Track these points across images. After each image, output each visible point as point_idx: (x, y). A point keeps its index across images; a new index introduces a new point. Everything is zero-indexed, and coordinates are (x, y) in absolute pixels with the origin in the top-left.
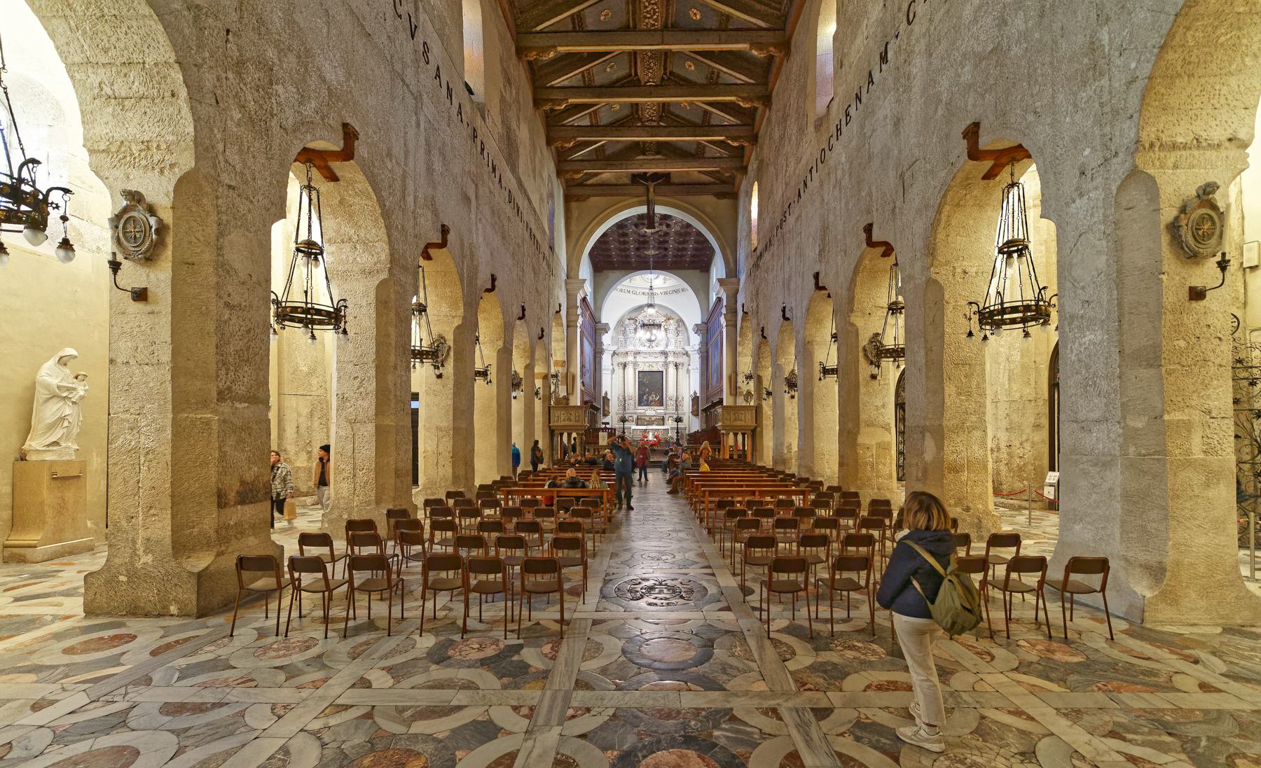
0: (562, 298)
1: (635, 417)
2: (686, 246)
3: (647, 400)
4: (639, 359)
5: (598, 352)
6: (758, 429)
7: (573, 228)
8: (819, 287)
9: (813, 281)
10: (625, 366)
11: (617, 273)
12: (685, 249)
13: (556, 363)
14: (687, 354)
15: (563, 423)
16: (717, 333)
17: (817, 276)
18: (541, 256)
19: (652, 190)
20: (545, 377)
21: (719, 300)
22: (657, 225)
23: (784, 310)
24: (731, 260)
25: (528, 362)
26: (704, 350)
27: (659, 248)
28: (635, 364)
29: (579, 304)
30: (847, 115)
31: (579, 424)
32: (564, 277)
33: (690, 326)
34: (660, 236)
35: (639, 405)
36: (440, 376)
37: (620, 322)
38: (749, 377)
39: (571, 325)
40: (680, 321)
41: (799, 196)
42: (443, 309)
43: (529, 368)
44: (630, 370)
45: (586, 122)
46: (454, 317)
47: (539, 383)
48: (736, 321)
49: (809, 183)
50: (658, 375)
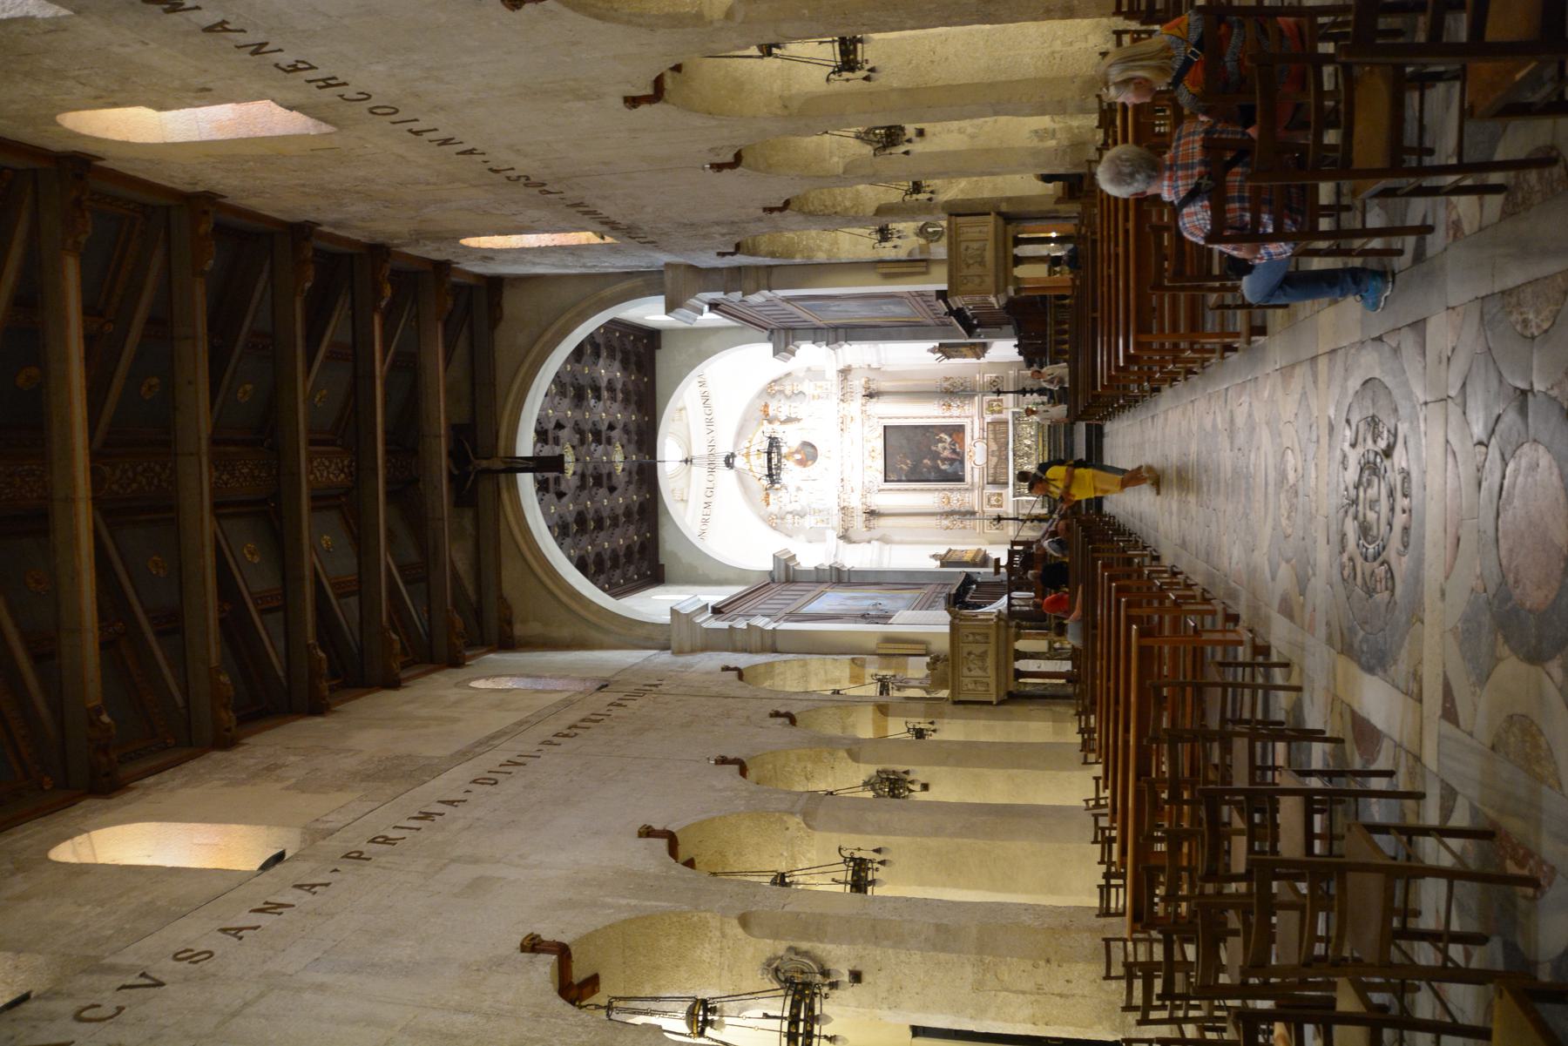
0: (713, 661)
1: (990, 490)
2: (604, 384)
3: (952, 461)
5: (838, 578)
6: (1004, 208)
7: (565, 633)
8: (658, 92)
9: (644, 109)
10: (872, 514)
11: (665, 534)
12: (611, 387)
13: (856, 679)
14: (845, 372)
15: (991, 672)
16: (789, 307)
17: (633, 102)
18: (616, 712)
19: (484, 464)
20: (883, 710)
21: (714, 306)
22: (557, 451)
23: (718, 167)
24: (626, 285)
25: (843, 754)
26: (832, 335)
27: (609, 441)
29: (725, 625)
30: (294, 68)
31: (992, 633)
32: (665, 657)
33: (778, 367)
34: (582, 441)
35: (961, 479)
36: (856, 977)
37: (775, 522)
38: (884, 234)
39: (771, 643)
40: (773, 389)
41: (471, 152)
42: (705, 957)
43: (855, 751)
45: (353, 601)
46: (724, 935)
47: (897, 728)
48: (757, 268)
49: (442, 135)
50: (892, 441)
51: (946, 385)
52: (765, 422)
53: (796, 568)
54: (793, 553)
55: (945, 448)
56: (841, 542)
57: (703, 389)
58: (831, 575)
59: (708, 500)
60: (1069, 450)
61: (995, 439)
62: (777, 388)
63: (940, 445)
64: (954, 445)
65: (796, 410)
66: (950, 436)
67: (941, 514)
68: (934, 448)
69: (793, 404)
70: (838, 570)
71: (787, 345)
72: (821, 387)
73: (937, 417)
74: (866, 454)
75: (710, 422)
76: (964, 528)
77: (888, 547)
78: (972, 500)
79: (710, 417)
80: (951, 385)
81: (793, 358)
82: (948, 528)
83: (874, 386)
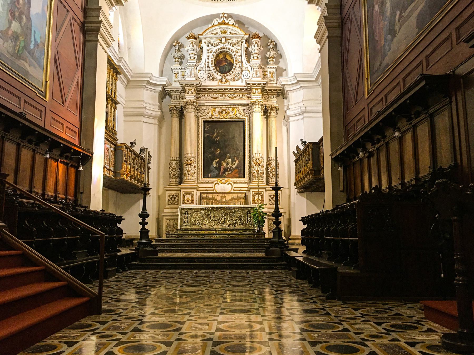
1: (197, 195)
3: (218, 168)
4: (205, 100)
10: (181, 113)
26: (335, 22)
28: (198, 108)
44: (190, 117)
52: (247, 36)
55: (228, 164)
56: (160, 88)
58: (91, 22)
63: (230, 160)
65: (256, 58)
66: (236, 167)
67: (180, 161)
68: (228, 156)
69: (260, 56)
70: (97, 30)
72: (272, 77)
74: (224, 108)
76: (170, 177)
77: (156, 121)
78: (190, 181)
82: (170, 165)
83: (273, 113)
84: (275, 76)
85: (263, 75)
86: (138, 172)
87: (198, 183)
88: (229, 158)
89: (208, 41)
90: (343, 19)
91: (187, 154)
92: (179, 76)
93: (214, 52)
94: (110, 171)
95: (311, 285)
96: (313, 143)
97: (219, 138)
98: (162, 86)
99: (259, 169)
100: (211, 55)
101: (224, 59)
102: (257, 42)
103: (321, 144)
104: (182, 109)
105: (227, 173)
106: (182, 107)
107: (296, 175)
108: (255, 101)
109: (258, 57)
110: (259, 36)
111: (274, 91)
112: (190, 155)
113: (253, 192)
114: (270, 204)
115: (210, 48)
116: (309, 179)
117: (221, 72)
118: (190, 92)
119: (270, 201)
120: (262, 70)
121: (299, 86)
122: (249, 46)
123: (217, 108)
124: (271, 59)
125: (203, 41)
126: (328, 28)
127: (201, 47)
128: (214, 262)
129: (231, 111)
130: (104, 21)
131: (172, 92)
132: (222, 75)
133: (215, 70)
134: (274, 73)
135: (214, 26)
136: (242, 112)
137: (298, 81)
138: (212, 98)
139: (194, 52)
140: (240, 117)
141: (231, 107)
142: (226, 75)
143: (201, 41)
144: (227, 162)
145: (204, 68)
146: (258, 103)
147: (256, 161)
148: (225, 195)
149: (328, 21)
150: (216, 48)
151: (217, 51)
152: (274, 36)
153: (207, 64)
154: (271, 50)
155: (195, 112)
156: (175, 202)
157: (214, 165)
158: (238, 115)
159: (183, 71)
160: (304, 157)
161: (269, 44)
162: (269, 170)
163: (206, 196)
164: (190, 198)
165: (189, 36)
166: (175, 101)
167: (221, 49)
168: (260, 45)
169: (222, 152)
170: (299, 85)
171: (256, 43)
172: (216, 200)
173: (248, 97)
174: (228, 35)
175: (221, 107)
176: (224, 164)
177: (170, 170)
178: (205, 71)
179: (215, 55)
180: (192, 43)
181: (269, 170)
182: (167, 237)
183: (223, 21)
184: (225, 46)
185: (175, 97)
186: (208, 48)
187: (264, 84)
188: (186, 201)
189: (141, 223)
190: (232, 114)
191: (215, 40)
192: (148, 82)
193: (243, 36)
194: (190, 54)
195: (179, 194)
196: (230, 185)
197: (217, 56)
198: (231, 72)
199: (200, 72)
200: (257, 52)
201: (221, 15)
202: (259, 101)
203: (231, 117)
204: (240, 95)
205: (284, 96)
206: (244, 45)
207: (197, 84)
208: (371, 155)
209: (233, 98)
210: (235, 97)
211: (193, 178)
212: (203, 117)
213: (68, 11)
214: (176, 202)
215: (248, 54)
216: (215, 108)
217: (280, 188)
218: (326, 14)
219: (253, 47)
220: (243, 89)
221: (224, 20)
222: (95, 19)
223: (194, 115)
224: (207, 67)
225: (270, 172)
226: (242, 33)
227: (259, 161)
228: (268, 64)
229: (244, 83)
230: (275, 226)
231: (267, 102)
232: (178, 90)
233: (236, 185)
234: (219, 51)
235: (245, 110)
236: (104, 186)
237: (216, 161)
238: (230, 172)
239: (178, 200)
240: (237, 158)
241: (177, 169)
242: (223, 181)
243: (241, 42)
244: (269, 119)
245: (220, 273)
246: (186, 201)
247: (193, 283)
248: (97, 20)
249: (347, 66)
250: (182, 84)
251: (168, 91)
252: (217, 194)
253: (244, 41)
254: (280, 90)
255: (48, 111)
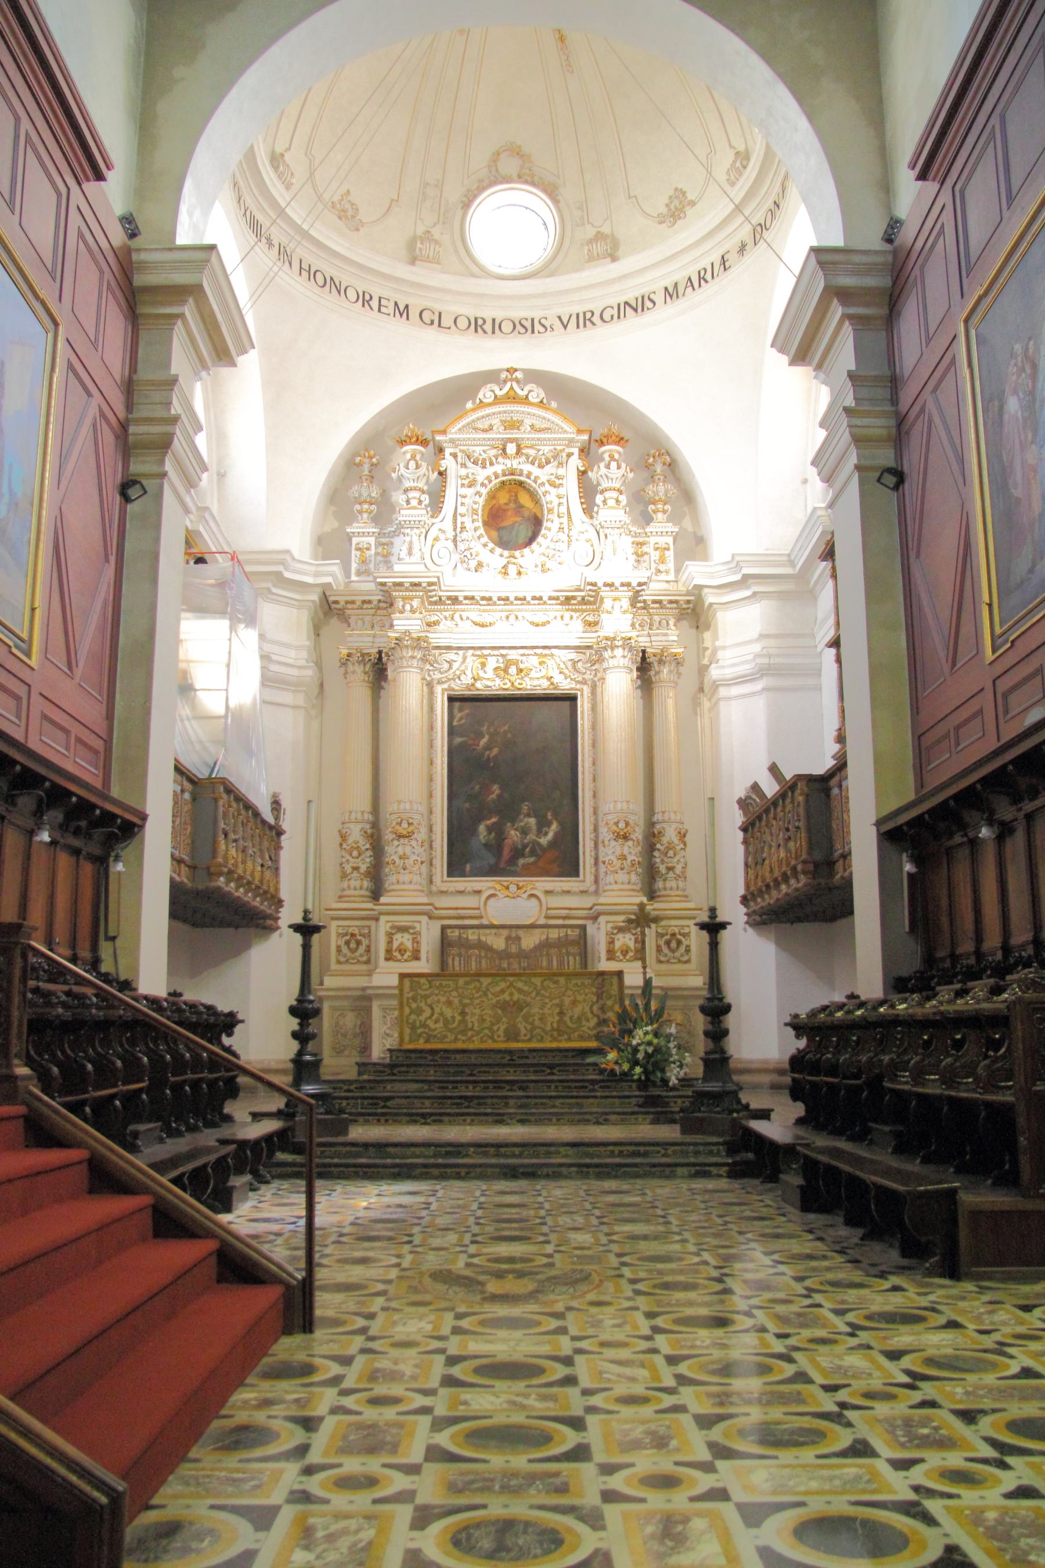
1: (429, 934)
3: (496, 846)
26: (879, 425)
50: (544, 712)
51: (670, 834)
53: (179, 330)
54: (241, 360)
55: (524, 832)
56: (315, 597)
57: (659, 298)
59: (414, 313)
60: (517, 1150)
61: (545, 945)
62: (659, 468)
63: (532, 821)
64: (533, 853)
65: (611, 503)
66: (553, 844)
67: (375, 825)
68: (525, 808)
69: (623, 499)
70: (164, 444)
71: (844, 295)
72: (662, 560)
73: (595, 812)
74: (513, 655)
75: (585, 320)
76: (344, 876)
77: (300, 700)
79: (596, 319)
80: (670, 847)
81: (785, 359)
84: (672, 558)
85: (636, 553)
86: (254, 862)
87: (430, 893)
88: (528, 815)
89: (463, 451)
90: (901, 421)
91: (399, 802)
92: (373, 559)
93: (482, 485)
94: (183, 865)
95: (860, 1232)
96: (810, 779)
97: (495, 751)
98: (320, 590)
99: (626, 849)
100: (472, 490)
101: (512, 505)
102: (616, 456)
103: (834, 782)
104: (380, 659)
105: (521, 861)
106: (380, 652)
107: (747, 873)
108: (612, 635)
109: (617, 501)
110: (622, 439)
111: (669, 606)
112: (408, 806)
113: (610, 925)
114: (660, 962)
115: (470, 471)
116: (797, 889)
117: (503, 543)
118: (408, 607)
119: (659, 949)
120: (630, 539)
121: (747, 593)
122: (590, 467)
123: (490, 655)
124: (660, 506)
125: (448, 452)
126: (858, 440)
127: (442, 469)
128: (530, 1157)
129: (537, 665)
130: (183, 417)
131: (349, 606)
132: (506, 553)
133: (485, 539)
134: (668, 549)
135: (482, 405)
136: (570, 668)
137: (746, 578)
138: (476, 624)
139: (421, 484)
140: (565, 685)
141: (536, 654)
142: (517, 553)
143: (441, 450)
144: (522, 828)
145: (451, 534)
146: (620, 643)
147: (617, 824)
148: (521, 933)
149: (858, 422)
150: (490, 471)
151: (490, 481)
152: (667, 437)
153: (459, 519)
154: (656, 478)
155: (422, 669)
156: (357, 954)
157: (481, 837)
158: (558, 679)
159: (383, 540)
160: (775, 818)
161: (651, 460)
162: (656, 854)
163: (460, 937)
164: (409, 945)
165: (407, 436)
166: (359, 635)
167: (504, 475)
168: (623, 465)
169: (506, 795)
170: (748, 588)
171: (612, 458)
172: (489, 949)
173: (589, 624)
174: (524, 434)
175: (503, 652)
176: (513, 832)
177: (344, 853)
178: (455, 541)
179: (484, 491)
180: (413, 457)
181: (656, 854)
182: (360, 1074)
183: (512, 393)
184: (515, 466)
185: (360, 622)
186: (463, 472)
187: (640, 584)
188: (396, 954)
189: (295, 1035)
190: (539, 675)
191: (485, 448)
192: (279, 579)
193: (572, 436)
194: (406, 491)
195: (373, 928)
196: (534, 900)
197: (492, 496)
198: (534, 545)
199: (438, 545)
200: (617, 485)
201: (504, 375)
202: (623, 635)
203: (535, 682)
204: (562, 617)
205: (697, 622)
206: (575, 462)
207: (430, 584)
208: (1005, 830)
209: (543, 624)
210: (549, 622)
211: (416, 878)
212: (446, 686)
213: (89, 394)
214: (361, 956)
215: (588, 492)
216: (485, 656)
217: (723, 926)
218: (850, 401)
219: (603, 470)
220: (574, 598)
221: (512, 388)
222: (159, 413)
223: (419, 677)
224: (459, 530)
225: (658, 860)
226: (569, 430)
227: (627, 824)
228: (648, 520)
229: (575, 581)
230: (711, 1045)
231: (648, 639)
232: (370, 602)
233: (554, 902)
234: (498, 480)
235: (580, 665)
236: (173, 915)
237: (488, 822)
238: (532, 860)
239: (368, 950)
240: (556, 815)
241: (363, 848)
242: (513, 888)
243: (564, 455)
244: (655, 692)
245: (558, 1192)
246: (396, 954)
247: (503, 1229)
248: (164, 414)
249: (918, 556)
250: (383, 584)
251: (336, 602)
252: (493, 931)
253: (576, 451)
254: (688, 602)
255: (35, 698)
